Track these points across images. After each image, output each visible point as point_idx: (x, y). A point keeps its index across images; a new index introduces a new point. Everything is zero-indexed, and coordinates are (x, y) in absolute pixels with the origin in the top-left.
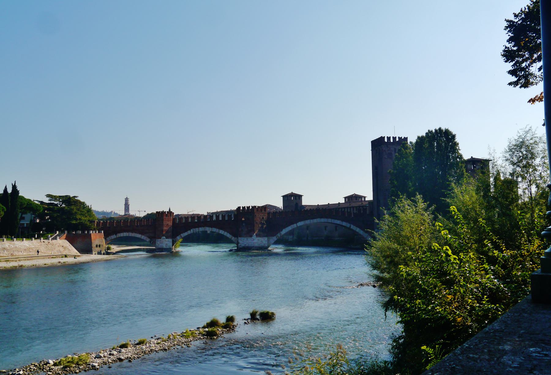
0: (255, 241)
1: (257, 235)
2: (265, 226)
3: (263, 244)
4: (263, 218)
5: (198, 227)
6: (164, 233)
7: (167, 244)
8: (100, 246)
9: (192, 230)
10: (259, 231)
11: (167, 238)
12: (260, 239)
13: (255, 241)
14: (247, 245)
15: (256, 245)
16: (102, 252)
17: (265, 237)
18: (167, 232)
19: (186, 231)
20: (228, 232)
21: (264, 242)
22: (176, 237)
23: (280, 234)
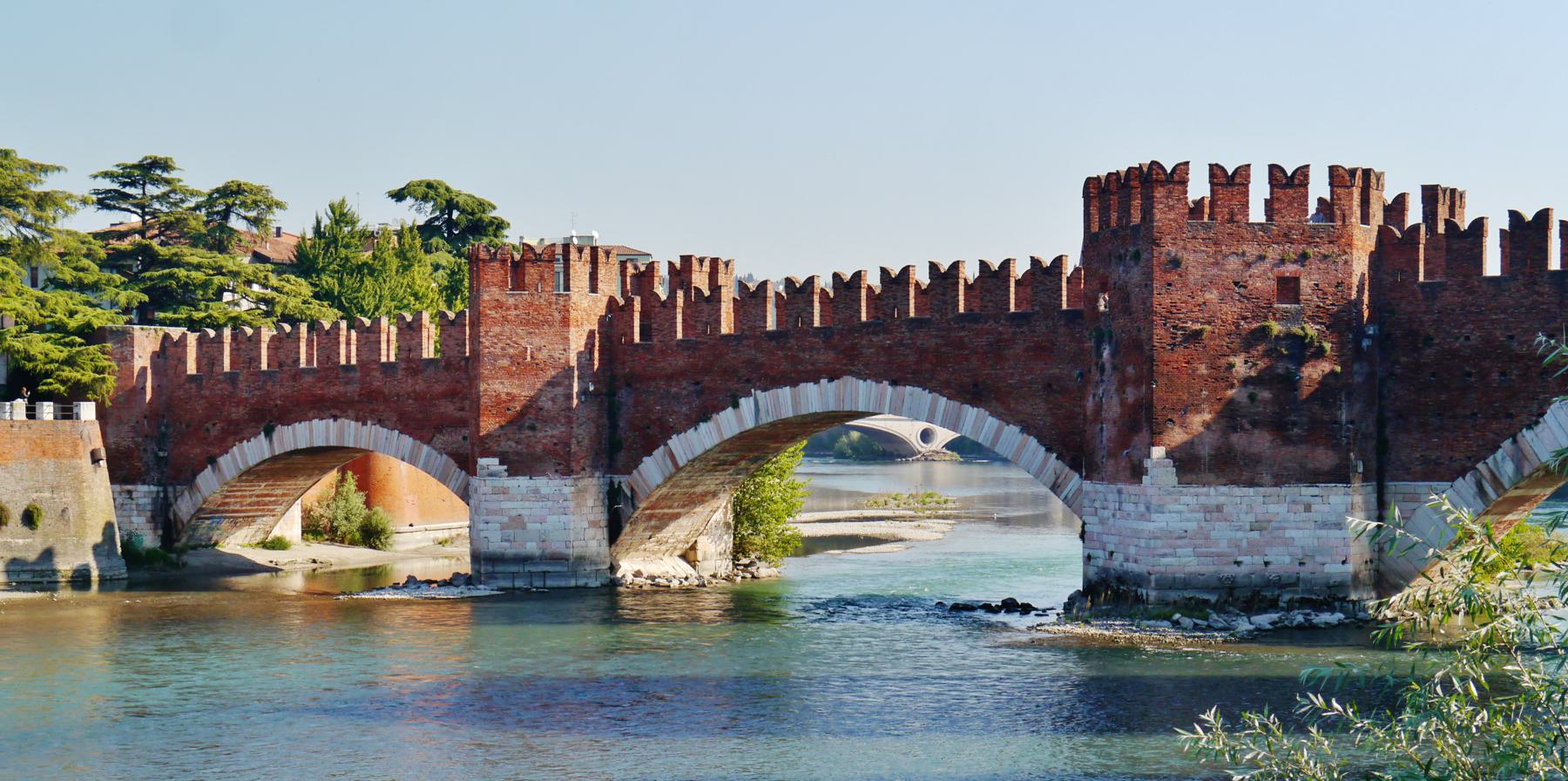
0: (1159, 522)
1: (1187, 464)
2: (1314, 372)
3: (1281, 562)
4: (1288, 288)
5: (794, 383)
6: (489, 425)
7: (518, 522)
8: (29, 518)
9: (746, 404)
10: (1230, 416)
11: (518, 465)
12: (1243, 503)
13: (1159, 522)
14: (1116, 563)
15: (1185, 562)
16: (65, 566)
17: (1314, 477)
18: (525, 417)
19: (704, 415)
20: (1026, 429)
21: (1303, 537)
22: (636, 463)
23: (1519, 458)
